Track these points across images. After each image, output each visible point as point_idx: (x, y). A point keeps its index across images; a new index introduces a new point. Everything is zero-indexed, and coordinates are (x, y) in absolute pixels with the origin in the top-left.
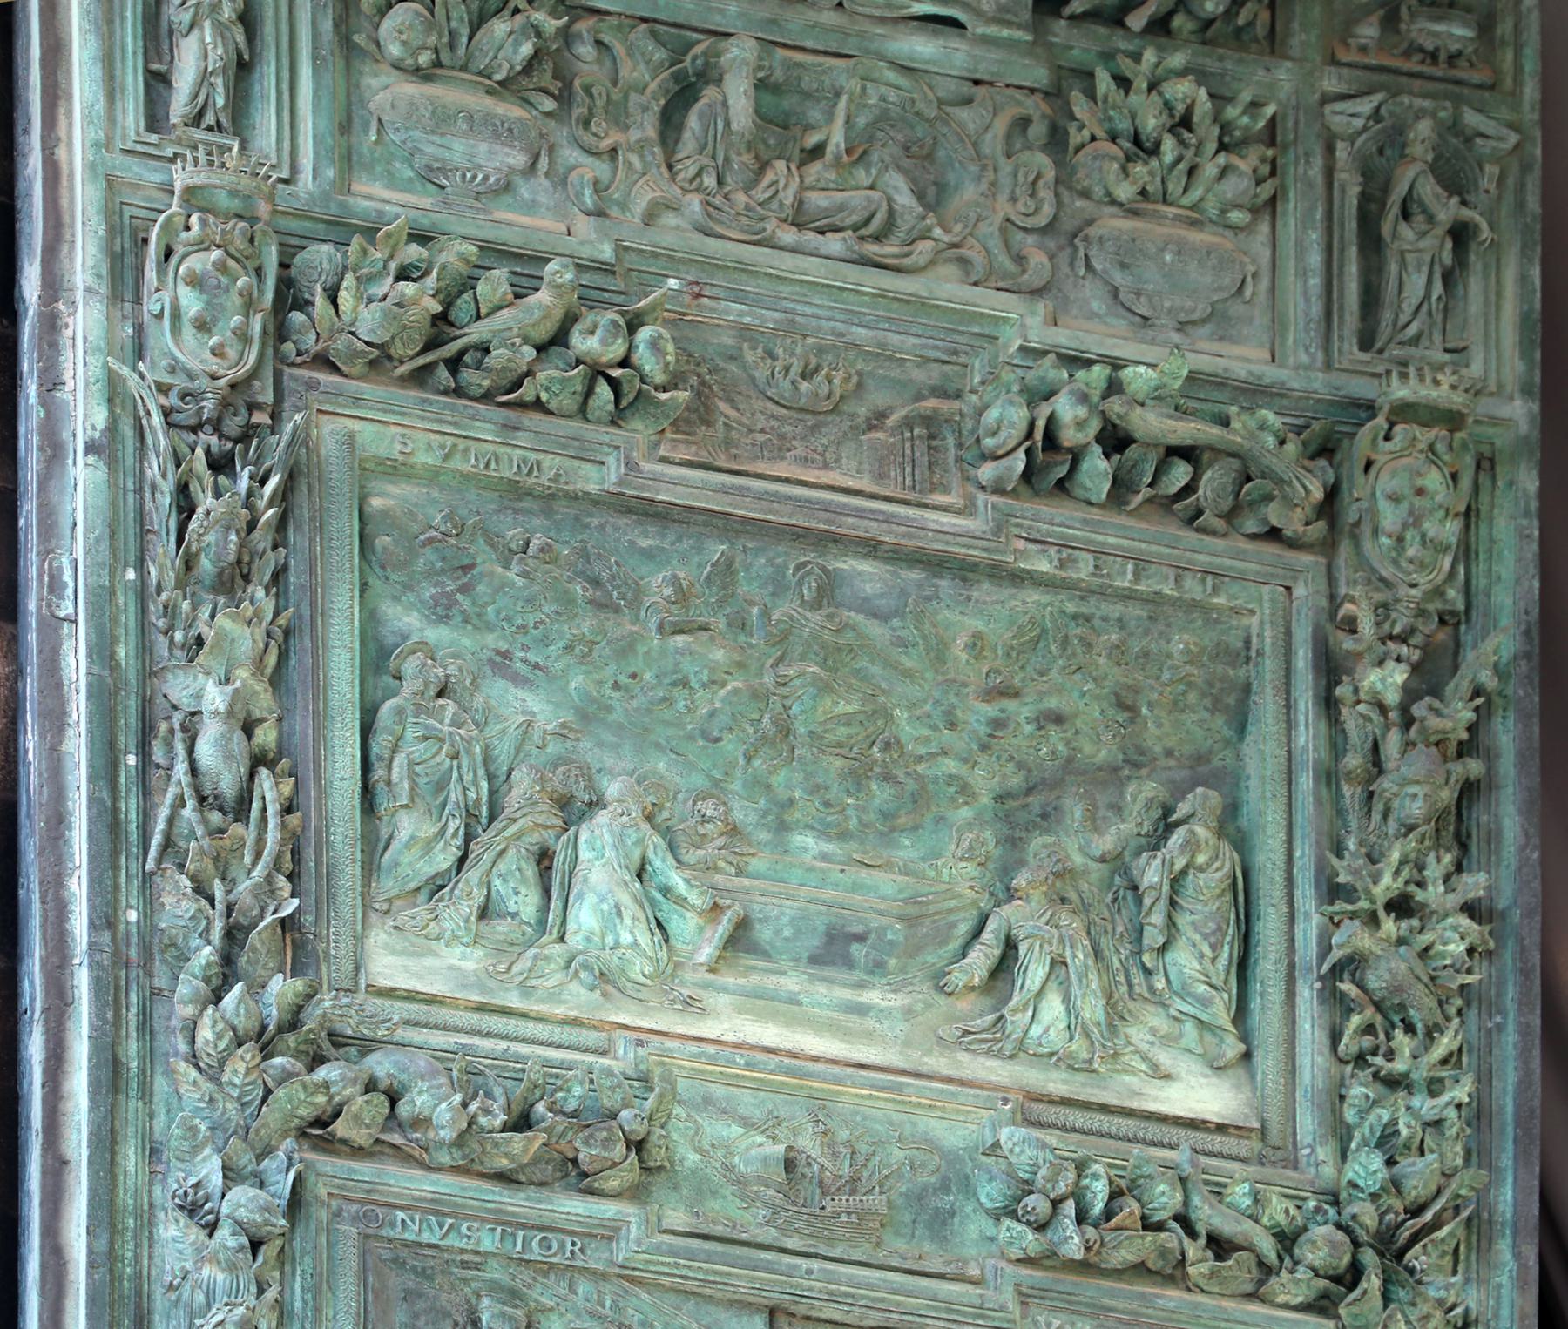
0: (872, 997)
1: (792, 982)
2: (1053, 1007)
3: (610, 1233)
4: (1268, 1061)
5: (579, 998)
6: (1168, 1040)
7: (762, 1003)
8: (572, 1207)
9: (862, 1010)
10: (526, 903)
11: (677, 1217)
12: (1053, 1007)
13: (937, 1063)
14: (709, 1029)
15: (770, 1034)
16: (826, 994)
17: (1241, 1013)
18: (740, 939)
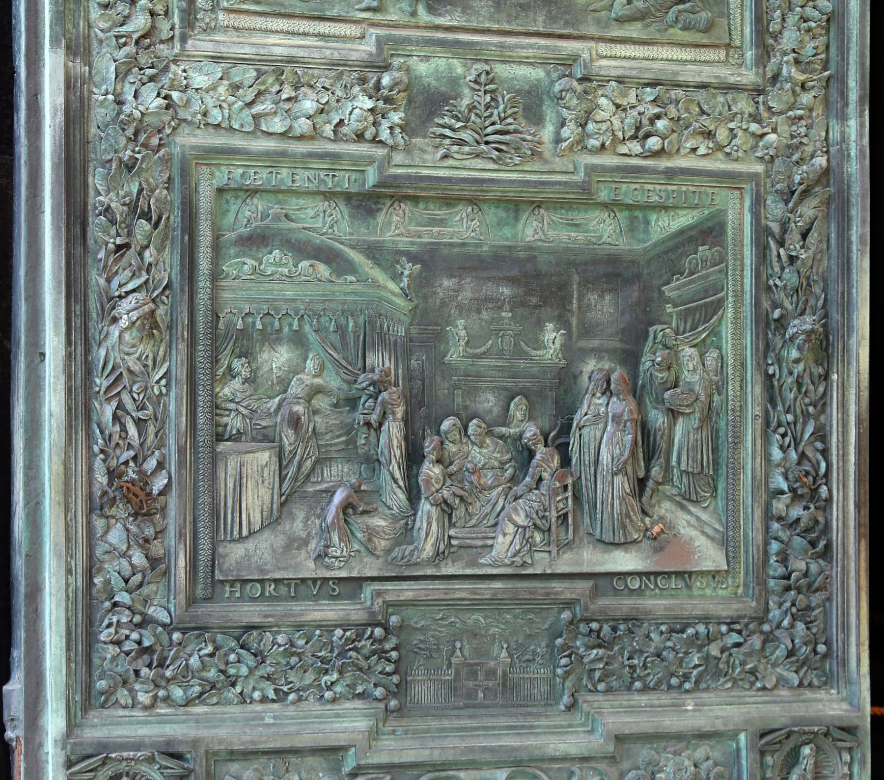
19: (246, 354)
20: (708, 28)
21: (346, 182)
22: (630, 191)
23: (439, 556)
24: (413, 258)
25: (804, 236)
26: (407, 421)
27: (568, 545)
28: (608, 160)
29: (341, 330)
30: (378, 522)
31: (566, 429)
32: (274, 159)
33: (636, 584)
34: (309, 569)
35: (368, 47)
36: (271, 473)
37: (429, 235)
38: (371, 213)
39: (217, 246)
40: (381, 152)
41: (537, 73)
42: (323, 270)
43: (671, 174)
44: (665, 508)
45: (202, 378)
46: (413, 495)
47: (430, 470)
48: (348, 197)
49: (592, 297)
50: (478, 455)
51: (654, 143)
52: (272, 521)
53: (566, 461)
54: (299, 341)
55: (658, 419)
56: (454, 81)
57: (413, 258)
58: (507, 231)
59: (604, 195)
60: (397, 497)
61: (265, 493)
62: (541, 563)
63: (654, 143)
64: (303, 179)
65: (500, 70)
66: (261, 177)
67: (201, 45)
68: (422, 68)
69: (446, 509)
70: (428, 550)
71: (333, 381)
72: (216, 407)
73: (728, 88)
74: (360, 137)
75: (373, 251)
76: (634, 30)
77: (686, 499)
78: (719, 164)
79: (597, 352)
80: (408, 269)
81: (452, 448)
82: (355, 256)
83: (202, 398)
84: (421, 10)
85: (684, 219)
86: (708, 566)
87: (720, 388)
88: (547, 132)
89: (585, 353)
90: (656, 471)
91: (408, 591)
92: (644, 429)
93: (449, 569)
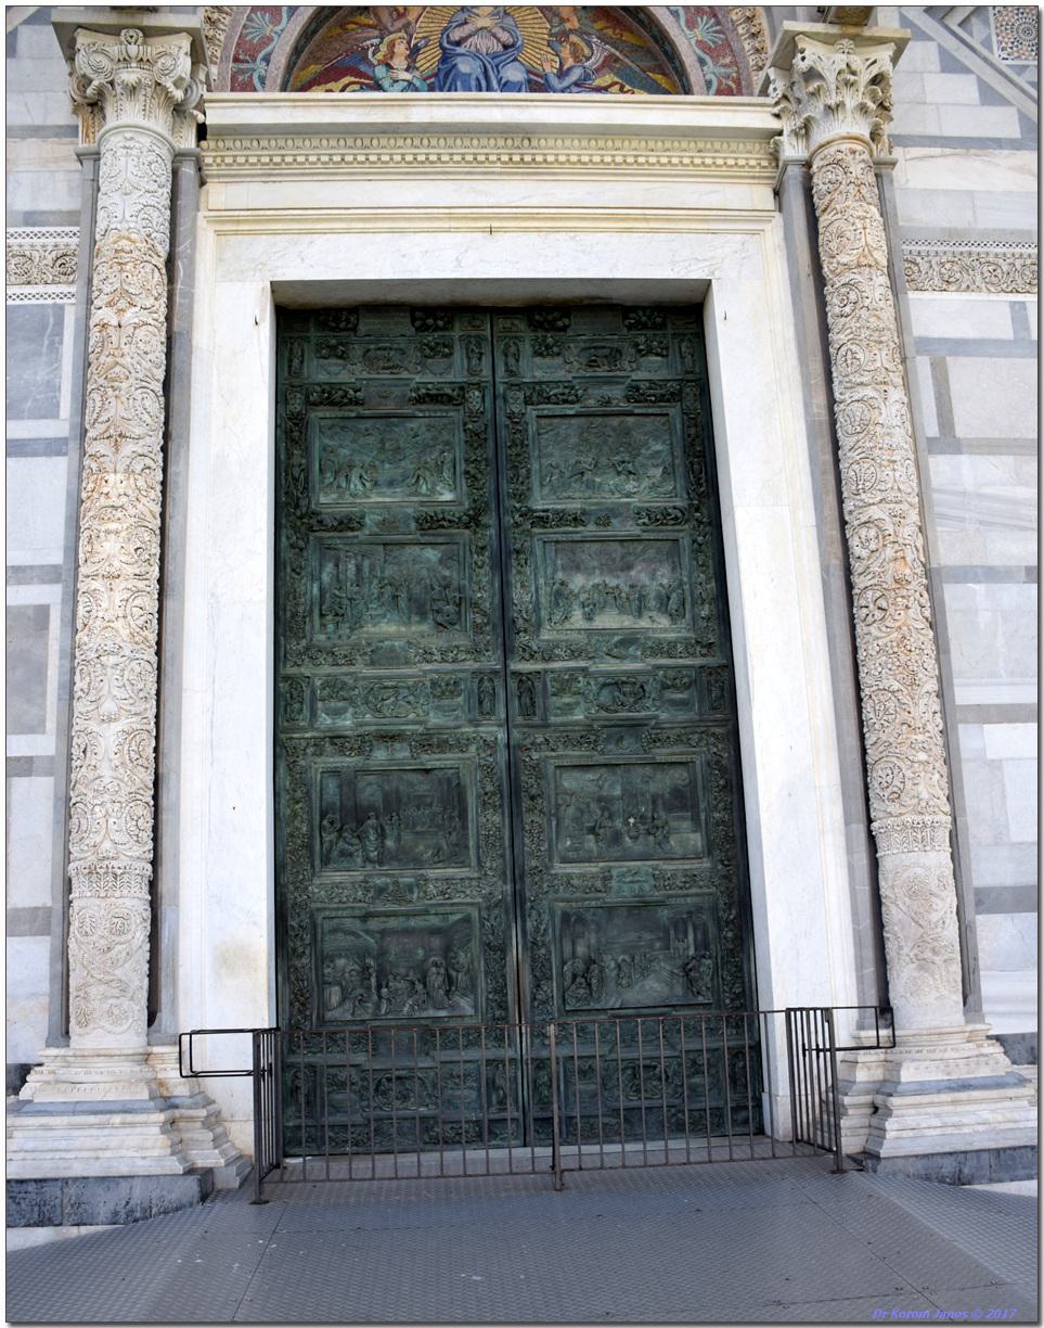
0: (398, 490)
1: (385, 490)
2: (424, 487)
3: (357, 537)
4: (458, 488)
5: (351, 500)
6: (443, 488)
7: (379, 494)
8: (350, 534)
9: (395, 492)
10: (344, 485)
11: (367, 532)
12: (424, 487)
13: (406, 499)
14: (372, 500)
15: (380, 500)
16: (389, 491)
17: (454, 482)
18: (376, 484)
19: (332, 961)
20: (462, 863)
21: (357, 913)
22: (441, 910)
23: (387, 1013)
24: (378, 933)
25: (496, 918)
26: (377, 977)
27: (426, 1009)
28: (433, 902)
29: (358, 953)
30: (369, 1005)
31: (425, 977)
32: (338, 909)
33: (446, 1020)
34: (349, 1017)
35: (362, 878)
36: (339, 993)
37: (383, 926)
38: (366, 921)
39: (323, 933)
40: (365, 905)
41: (412, 880)
42: (352, 938)
43: (452, 905)
44: (456, 998)
45: (320, 968)
46: (380, 997)
47: (384, 990)
48: (359, 917)
49: (432, 940)
50: (399, 985)
51: (447, 896)
52: (340, 1004)
53: (425, 986)
54: (346, 957)
55: (454, 974)
56: (387, 884)
57: (378, 933)
58: (406, 923)
59: (433, 912)
60: (375, 998)
61: (338, 998)
62: (417, 1015)
63: (447, 896)
64: (345, 913)
65: (401, 880)
66: (334, 914)
67: (317, 881)
68: (378, 882)
69: (389, 1000)
70: (383, 1012)
71: (357, 967)
72: (323, 975)
73: (471, 879)
74: (360, 901)
75: (367, 932)
76: (440, 865)
77: (464, 995)
78: (468, 900)
79: (434, 955)
80: (378, 936)
81: (391, 984)
82: (361, 933)
83: (320, 973)
84: (377, 867)
85: (458, 917)
86: (469, 1014)
87: (472, 964)
88: (415, 895)
89: (430, 957)
90: (453, 988)
91: (377, 1023)
92: (449, 977)
93: (389, 1017)
